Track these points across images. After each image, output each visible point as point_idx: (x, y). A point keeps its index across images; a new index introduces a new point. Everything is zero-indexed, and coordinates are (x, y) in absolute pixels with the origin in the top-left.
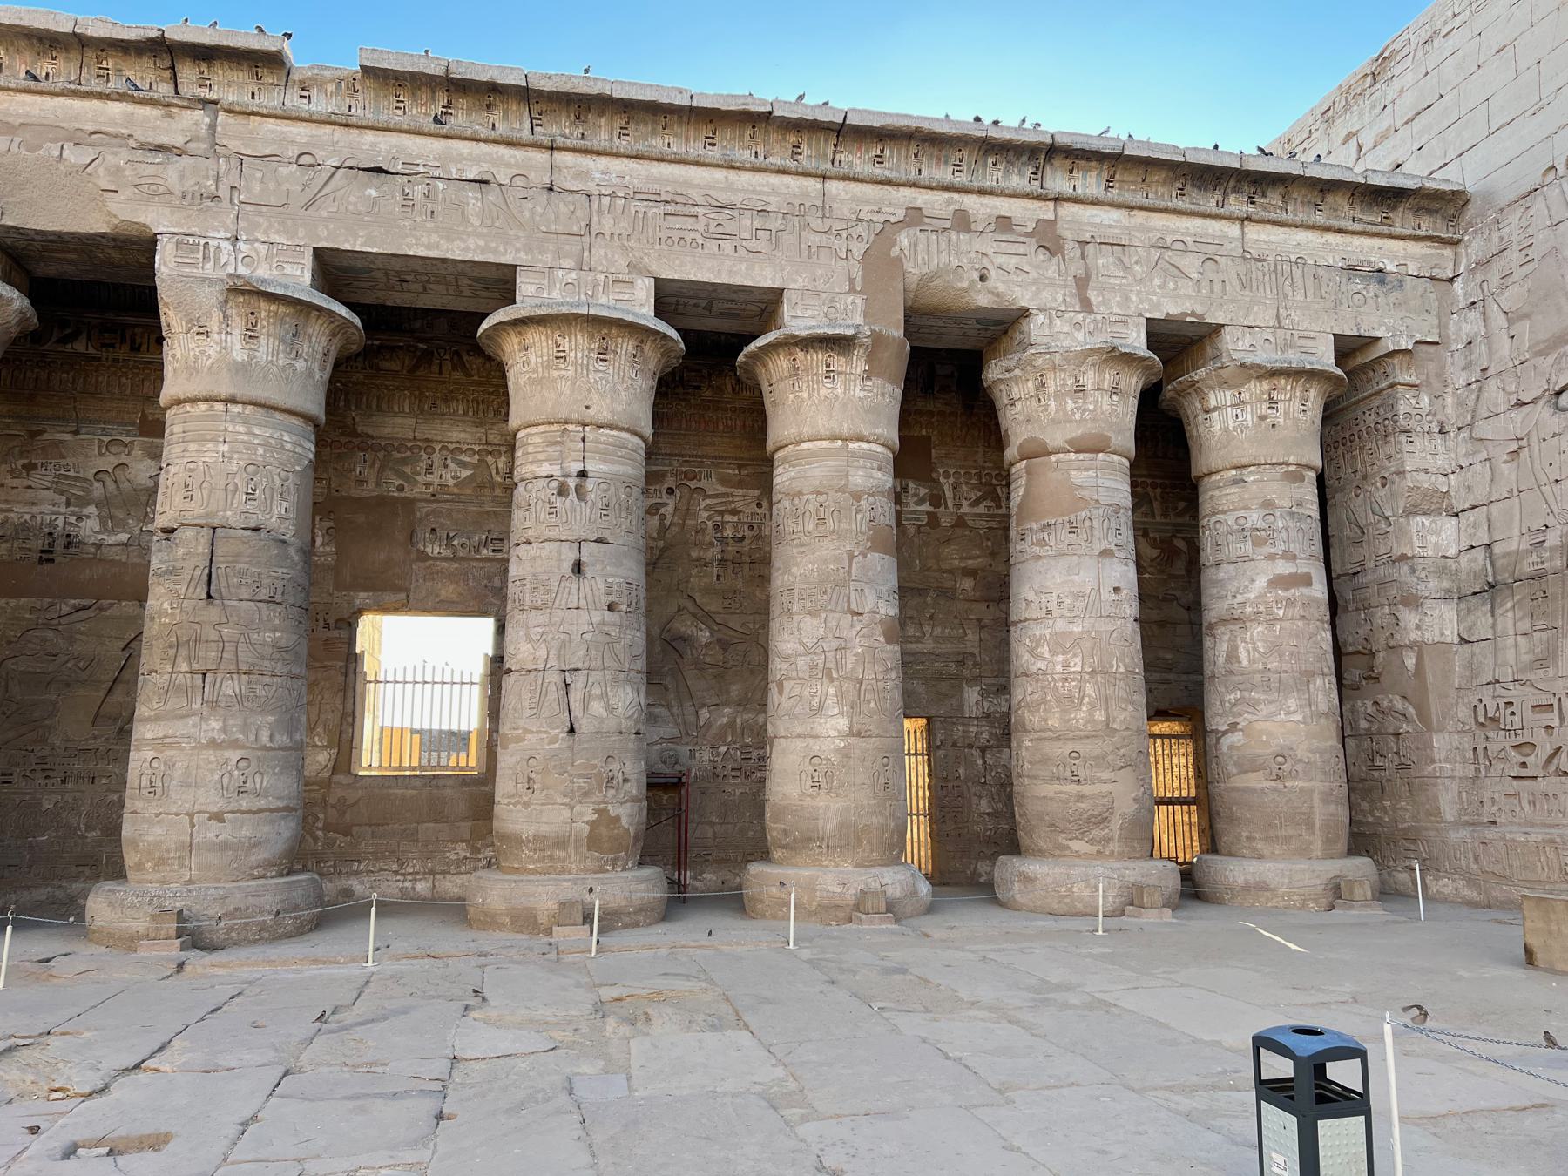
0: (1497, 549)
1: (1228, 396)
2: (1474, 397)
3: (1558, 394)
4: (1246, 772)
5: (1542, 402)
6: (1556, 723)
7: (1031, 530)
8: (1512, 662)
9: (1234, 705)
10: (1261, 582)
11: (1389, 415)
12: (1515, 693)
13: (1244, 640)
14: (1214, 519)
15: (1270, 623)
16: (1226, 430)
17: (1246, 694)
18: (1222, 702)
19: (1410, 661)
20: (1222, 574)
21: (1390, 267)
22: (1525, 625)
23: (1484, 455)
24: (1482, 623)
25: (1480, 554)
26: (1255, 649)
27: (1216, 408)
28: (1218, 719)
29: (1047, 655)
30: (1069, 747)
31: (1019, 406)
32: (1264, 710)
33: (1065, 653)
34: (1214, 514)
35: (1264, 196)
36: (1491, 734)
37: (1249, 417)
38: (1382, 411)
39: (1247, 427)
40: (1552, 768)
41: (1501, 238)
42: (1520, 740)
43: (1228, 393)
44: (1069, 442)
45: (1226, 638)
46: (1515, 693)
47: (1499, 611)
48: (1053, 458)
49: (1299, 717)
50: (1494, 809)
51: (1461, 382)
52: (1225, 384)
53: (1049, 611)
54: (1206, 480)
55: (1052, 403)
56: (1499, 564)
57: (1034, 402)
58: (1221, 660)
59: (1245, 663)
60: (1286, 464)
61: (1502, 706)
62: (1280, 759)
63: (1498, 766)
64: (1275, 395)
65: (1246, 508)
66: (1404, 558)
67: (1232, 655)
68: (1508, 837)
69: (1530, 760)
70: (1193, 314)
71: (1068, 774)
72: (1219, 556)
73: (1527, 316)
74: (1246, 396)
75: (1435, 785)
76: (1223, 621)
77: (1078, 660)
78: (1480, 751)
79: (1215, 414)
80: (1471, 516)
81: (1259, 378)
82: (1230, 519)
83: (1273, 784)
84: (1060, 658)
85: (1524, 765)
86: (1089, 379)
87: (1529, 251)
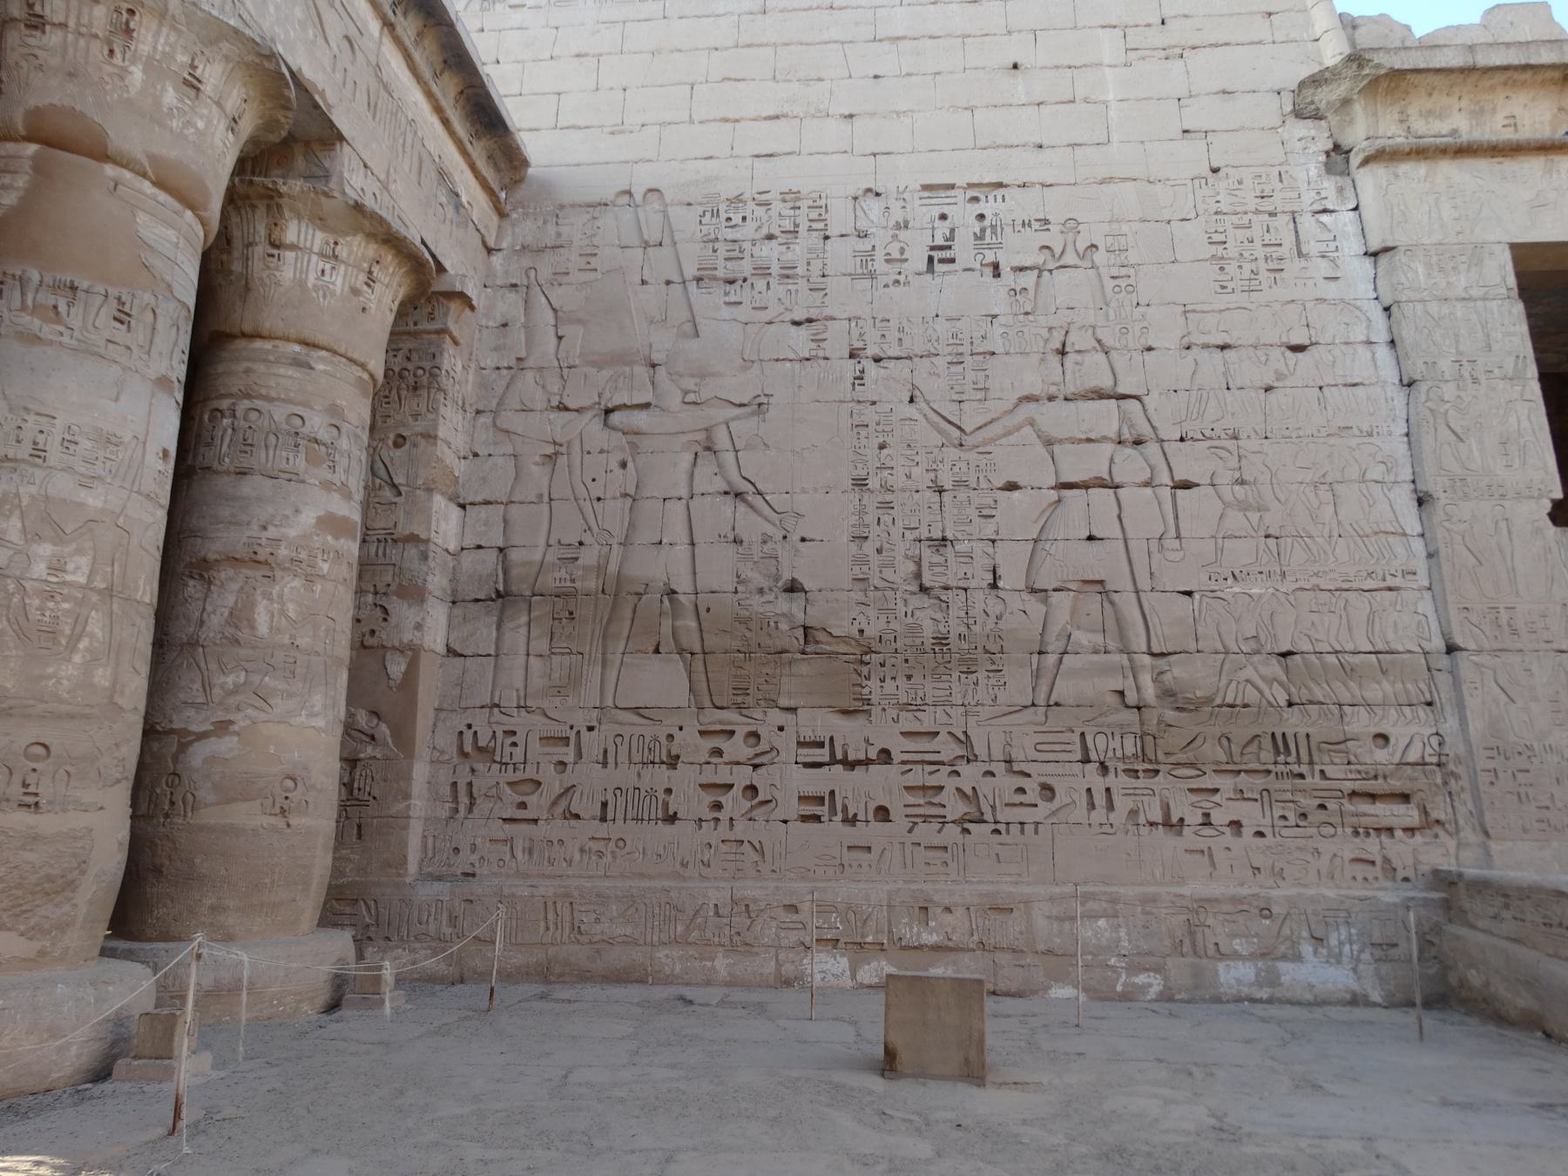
0: (514, 555)
1: (318, 239)
2: (504, 383)
3: (608, 412)
4: (234, 800)
5: (590, 414)
6: (570, 758)
7: (23, 282)
8: (519, 684)
9: (230, 693)
10: (308, 517)
11: (427, 365)
12: (519, 721)
13: (267, 596)
14: (245, 404)
15: (310, 579)
16: (302, 284)
17: (256, 679)
18: (206, 687)
19: (397, 668)
20: (248, 487)
21: (464, 199)
22: (541, 645)
23: (510, 450)
24: (483, 634)
25: (490, 559)
26: (283, 613)
27: (293, 247)
28: (191, 712)
29: (14, 535)
30: (32, 733)
31: (53, 38)
32: (280, 705)
33: (60, 538)
34: (248, 396)
35: (405, 14)
36: (480, 766)
37: (339, 281)
38: (415, 356)
39: (333, 294)
40: (559, 810)
41: (559, 235)
42: (519, 775)
43: (319, 235)
44: (152, 158)
45: (235, 586)
46: (519, 721)
47: (508, 625)
48: (110, 170)
49: (320, 722)
50: (475, 858)
51: (490, 361)
52: (320, 221)
53: (38, 452)
54: (240, 344)
55: (137, 74)
56: (514, 572)
57: (98, 51)
58: (215, 621)
59: (263, 629)
60: (363, 366)
61: (500, 735)
62: (290, 783)
63: (483, 806)
64: (376, 269)
65: (306, 405)
66: (413, 539)
67: (240, 616)
68: (506, 891)
69: (532, 800)
70: (322, 94)
71: (16, 790)
72: (245, 462)
73: (580, 321)
74: (342, 251)
75: (406, 828)
76: (234, 560)
77: (84, 562)
78: (462, 789)
79: (290, 255)
80: (483, 512)
81: (371, 236)
82: (279, 413)
83: (273, 820)
84: (46, 549)
85: (523, 805)
86: (212, 74)
87: (592, 260)
